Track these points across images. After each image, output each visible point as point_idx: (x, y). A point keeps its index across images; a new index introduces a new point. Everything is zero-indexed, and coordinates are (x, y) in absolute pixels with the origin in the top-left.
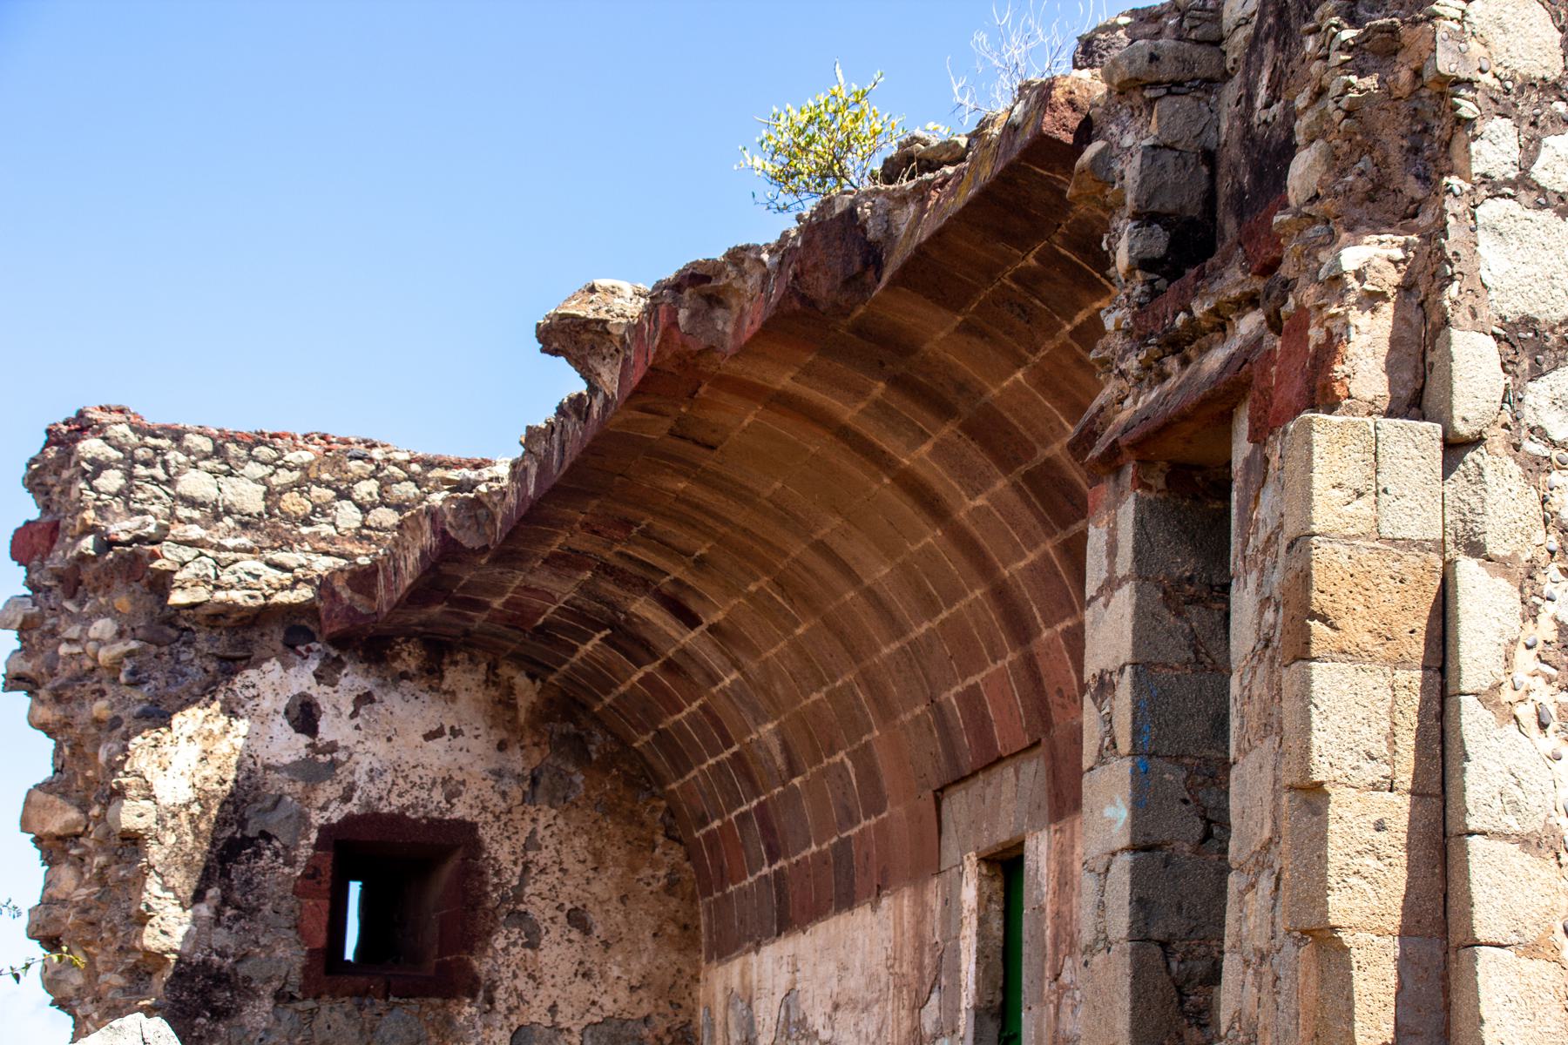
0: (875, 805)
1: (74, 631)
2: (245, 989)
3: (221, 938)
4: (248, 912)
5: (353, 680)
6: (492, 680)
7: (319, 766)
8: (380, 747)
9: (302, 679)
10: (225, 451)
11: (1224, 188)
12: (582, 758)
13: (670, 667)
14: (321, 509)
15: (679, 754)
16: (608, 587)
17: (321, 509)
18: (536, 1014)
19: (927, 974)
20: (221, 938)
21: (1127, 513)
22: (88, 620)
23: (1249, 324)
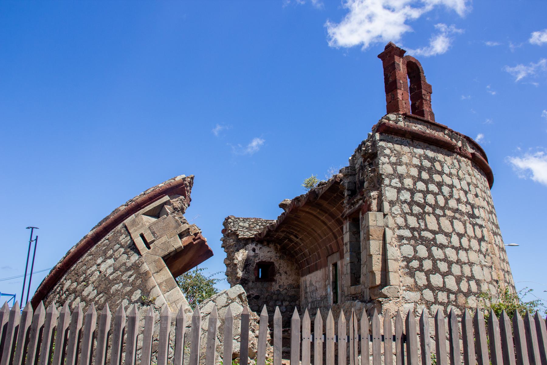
0: (320, 258)
2: (249, 281)
3: (246, 275)
4: (249, 272)
5: (259, 246)
6: (275, 245)
7: (256, 256)
9: (253, 246)
10: (244, 220)
11: (357, 186)
13: (295, 243)
16: (288, 234)
17: (255, 226)
18: (281, 283)
19: (327, 278)
20: (246, 275)
21: (348, 224)
23: (361, 202)
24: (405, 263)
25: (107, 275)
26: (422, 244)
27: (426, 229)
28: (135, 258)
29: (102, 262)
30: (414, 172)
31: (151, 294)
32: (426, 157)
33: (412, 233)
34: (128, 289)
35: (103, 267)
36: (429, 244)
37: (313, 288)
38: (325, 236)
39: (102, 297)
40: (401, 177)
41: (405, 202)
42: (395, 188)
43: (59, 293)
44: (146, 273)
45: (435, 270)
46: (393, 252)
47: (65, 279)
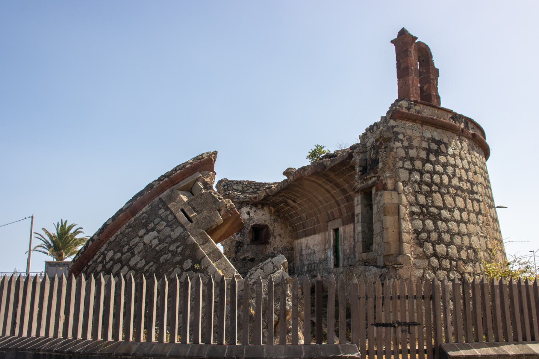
0: (318, 223)
2: (244, 244)
3: (241, 238)
4: (244, 235)
5: (254, 209)
6: (269, 208)
7: (250, 219)
8: (257, 216)
9: (248, 209)
11: (368, 163)
12: (280, 217)
13: (292, 207)
14: (248, 189)
15: (291, 216)
16: (286, 199)
17: (248, 189)
18: (276, 246)
19: (327, 241)
20: (241, 238)
21: (359, 197)
23: (374, 179)
24: (415, 235)
25: (153, 246)
26: (429, 219)
27: (433, 206)
29: (145, 234)
30: (423, 155)
32: (434, 140)
33: (421, 209)
34: (178, 258)
35: (146, 239)
36: (436, 218)
37: (310, 251)
38: (327, 202)
39: (152, 266)
40: (412, 160)
41: (416, 181)
42: (407, 169)
43: (101, 262)
44: (194, 244)
45: (440, 240)
46: (406, 226)
47: (106, 249)
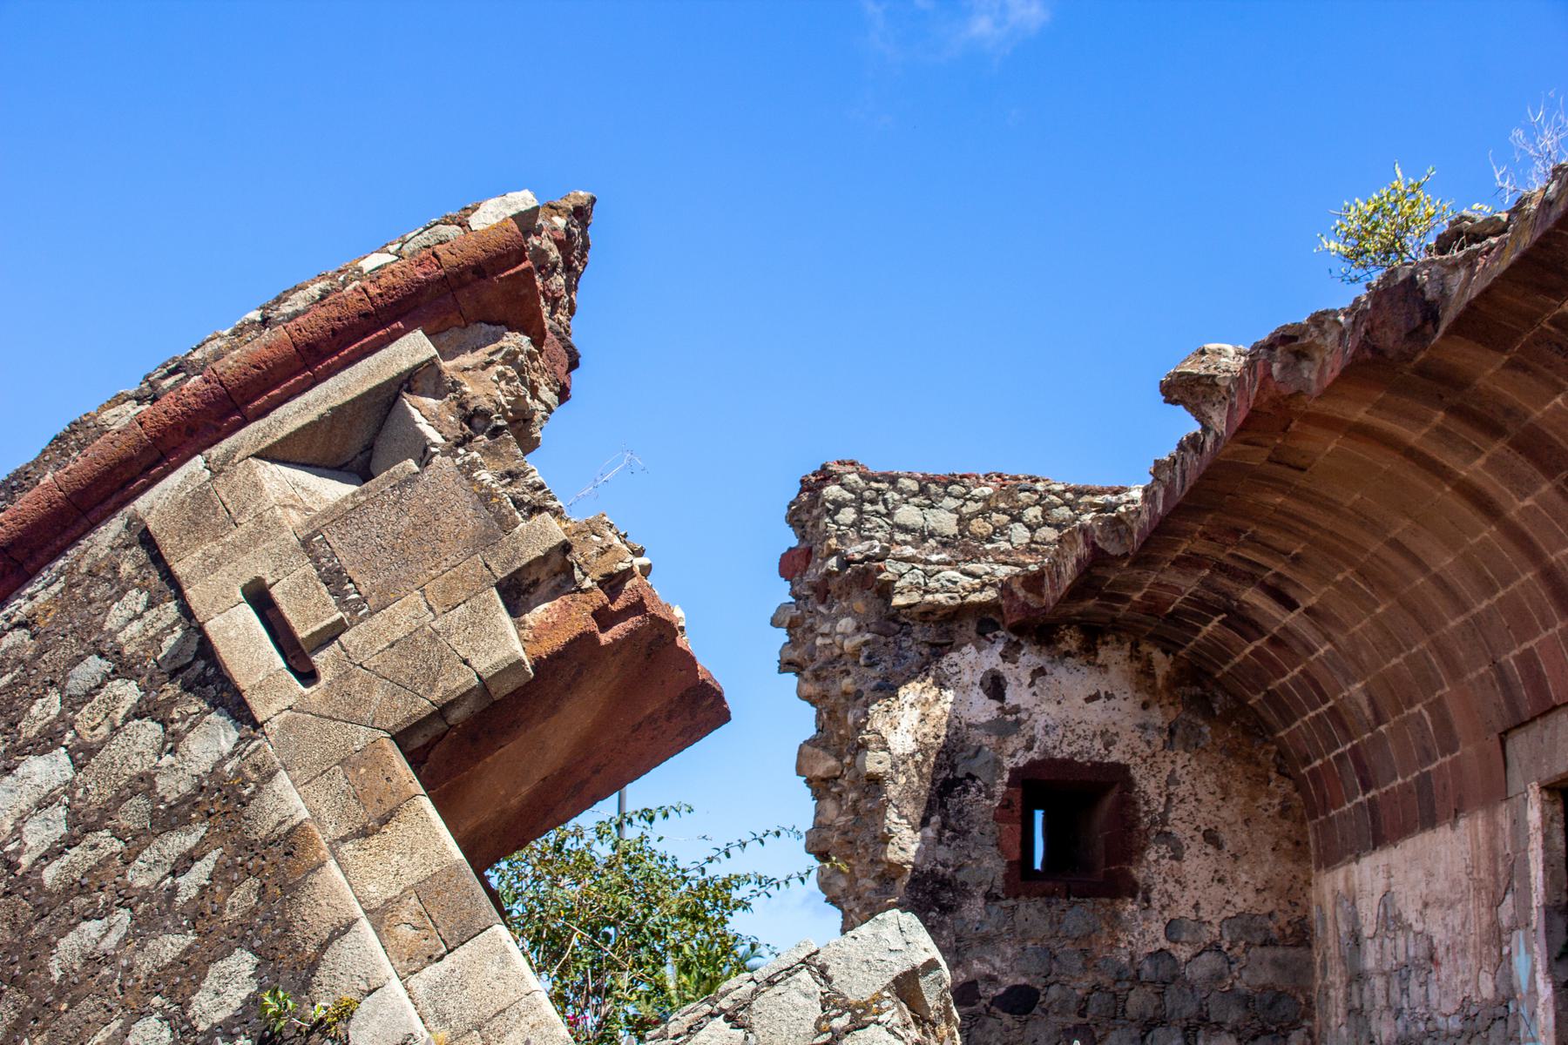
0: (1449, 746)
1: (826, 628)
2: (963, 891)
4: (961, 833)
5: (1030, 658)
6: (1135, 655)
8: (1052, 708)
9: (991, 658)
10: (928, 490)
12: (1208, 713)
13: (1275, 641)
14: (1000, 530)
15: (1285, 708)
16: (1223, 581)
17: (1000, 530)
18: (1183, 910)
20: (943, 853)
22: (836, 619)
25: (25, 861)
28: (211, 742)
31: (322, 974)
34: (171, 945)
37: (1404, 947)
38: (1489, 588)
44: (291, 841)
